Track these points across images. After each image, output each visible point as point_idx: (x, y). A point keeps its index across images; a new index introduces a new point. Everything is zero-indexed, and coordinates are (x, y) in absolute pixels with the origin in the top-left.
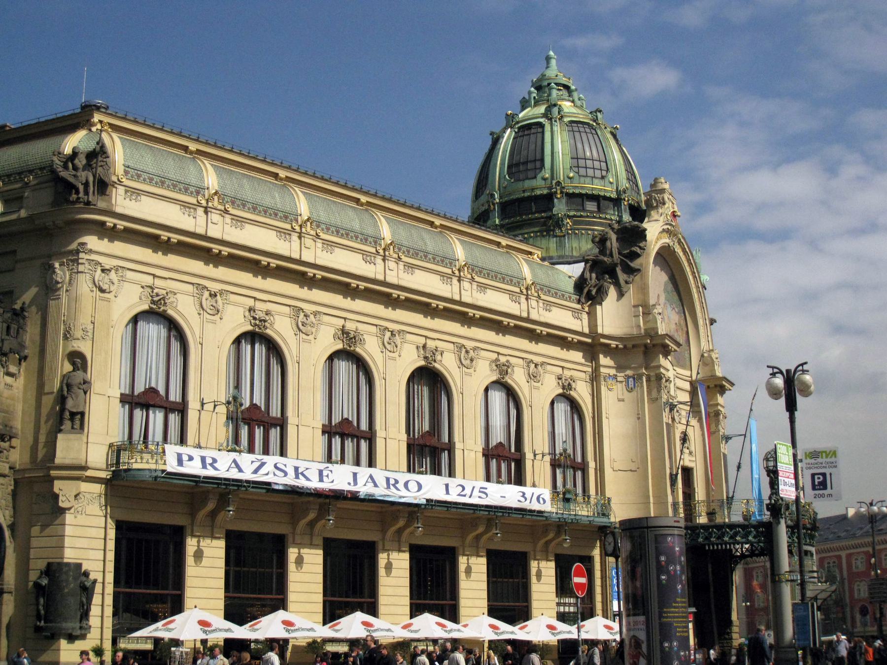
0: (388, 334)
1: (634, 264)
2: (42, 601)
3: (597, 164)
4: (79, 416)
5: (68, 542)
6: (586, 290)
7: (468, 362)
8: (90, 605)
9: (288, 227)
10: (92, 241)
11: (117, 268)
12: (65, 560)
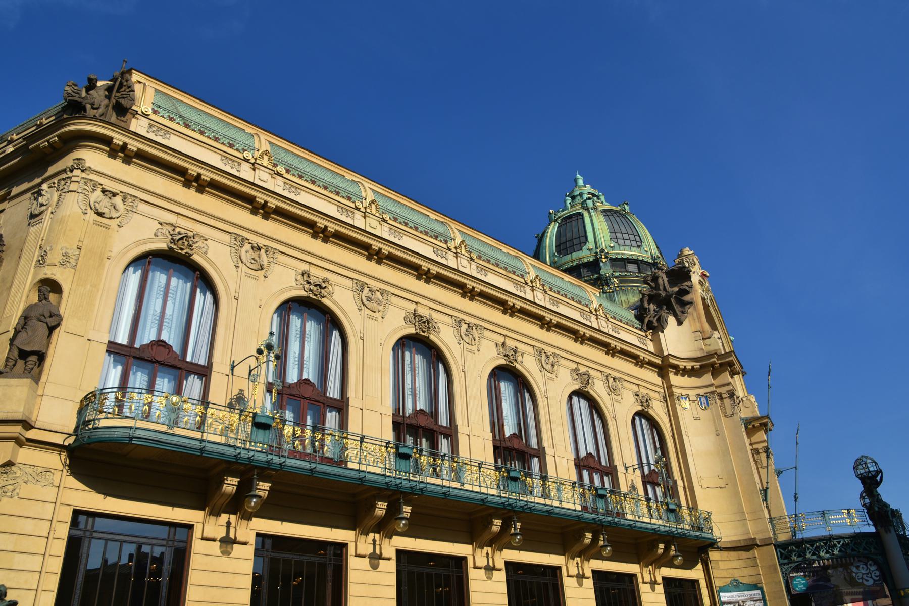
1: (687, 298)
3: (632, 237)
4: (34, 358)
6: (646, 321)
7: (548, 367)
9: (353, 205)
10: (93, 158)
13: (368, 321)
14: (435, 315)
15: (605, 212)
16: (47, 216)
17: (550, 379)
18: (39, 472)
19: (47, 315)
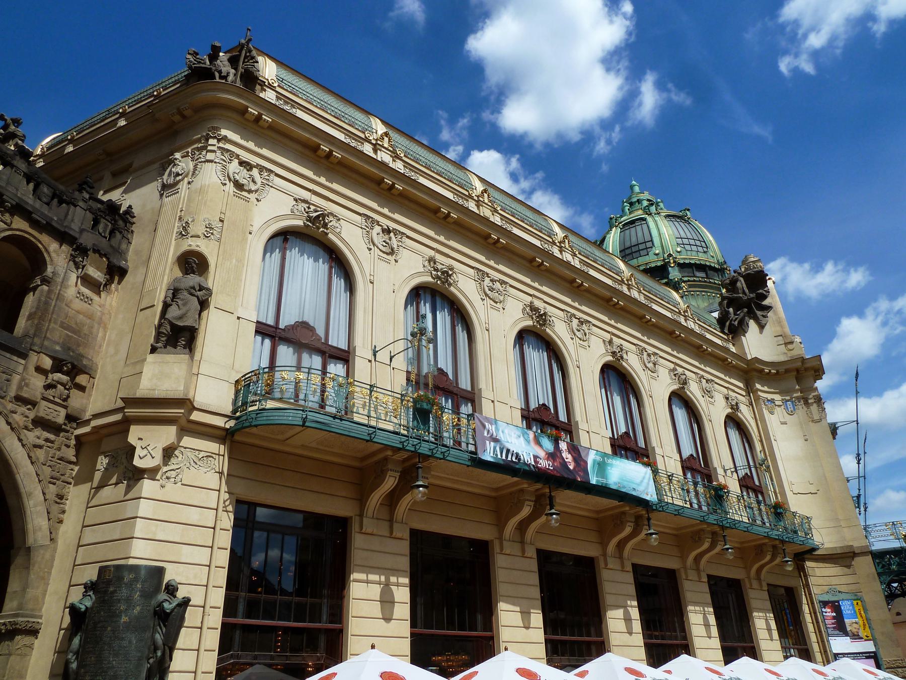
0: (575, 322)
1: (766, 302)
2: (76, 641)
3: (698, 243)
5: (140, 528)
6: (728, 324)
7: (650, 365)
8: (172, 649)
11: (261, 169)
12: (131, 562)
13: (491, 311)
14: (549, 309)
15: (667, 216)
16: (183, 186)
17: (653, 378)
18: (200, 456)
19: (197, 288)
